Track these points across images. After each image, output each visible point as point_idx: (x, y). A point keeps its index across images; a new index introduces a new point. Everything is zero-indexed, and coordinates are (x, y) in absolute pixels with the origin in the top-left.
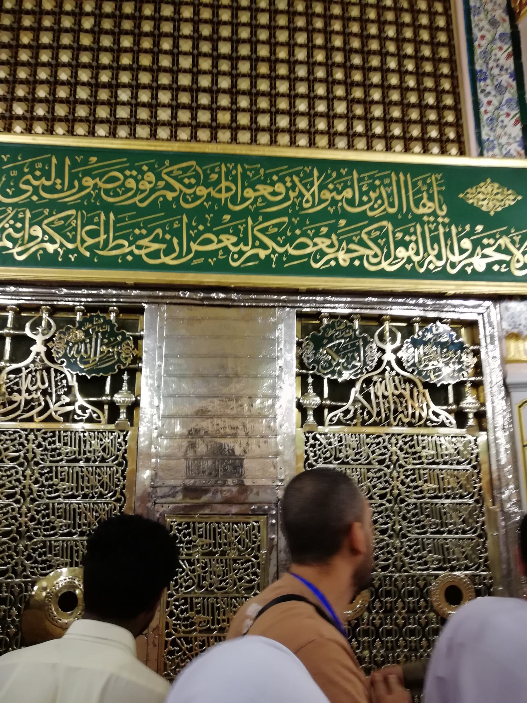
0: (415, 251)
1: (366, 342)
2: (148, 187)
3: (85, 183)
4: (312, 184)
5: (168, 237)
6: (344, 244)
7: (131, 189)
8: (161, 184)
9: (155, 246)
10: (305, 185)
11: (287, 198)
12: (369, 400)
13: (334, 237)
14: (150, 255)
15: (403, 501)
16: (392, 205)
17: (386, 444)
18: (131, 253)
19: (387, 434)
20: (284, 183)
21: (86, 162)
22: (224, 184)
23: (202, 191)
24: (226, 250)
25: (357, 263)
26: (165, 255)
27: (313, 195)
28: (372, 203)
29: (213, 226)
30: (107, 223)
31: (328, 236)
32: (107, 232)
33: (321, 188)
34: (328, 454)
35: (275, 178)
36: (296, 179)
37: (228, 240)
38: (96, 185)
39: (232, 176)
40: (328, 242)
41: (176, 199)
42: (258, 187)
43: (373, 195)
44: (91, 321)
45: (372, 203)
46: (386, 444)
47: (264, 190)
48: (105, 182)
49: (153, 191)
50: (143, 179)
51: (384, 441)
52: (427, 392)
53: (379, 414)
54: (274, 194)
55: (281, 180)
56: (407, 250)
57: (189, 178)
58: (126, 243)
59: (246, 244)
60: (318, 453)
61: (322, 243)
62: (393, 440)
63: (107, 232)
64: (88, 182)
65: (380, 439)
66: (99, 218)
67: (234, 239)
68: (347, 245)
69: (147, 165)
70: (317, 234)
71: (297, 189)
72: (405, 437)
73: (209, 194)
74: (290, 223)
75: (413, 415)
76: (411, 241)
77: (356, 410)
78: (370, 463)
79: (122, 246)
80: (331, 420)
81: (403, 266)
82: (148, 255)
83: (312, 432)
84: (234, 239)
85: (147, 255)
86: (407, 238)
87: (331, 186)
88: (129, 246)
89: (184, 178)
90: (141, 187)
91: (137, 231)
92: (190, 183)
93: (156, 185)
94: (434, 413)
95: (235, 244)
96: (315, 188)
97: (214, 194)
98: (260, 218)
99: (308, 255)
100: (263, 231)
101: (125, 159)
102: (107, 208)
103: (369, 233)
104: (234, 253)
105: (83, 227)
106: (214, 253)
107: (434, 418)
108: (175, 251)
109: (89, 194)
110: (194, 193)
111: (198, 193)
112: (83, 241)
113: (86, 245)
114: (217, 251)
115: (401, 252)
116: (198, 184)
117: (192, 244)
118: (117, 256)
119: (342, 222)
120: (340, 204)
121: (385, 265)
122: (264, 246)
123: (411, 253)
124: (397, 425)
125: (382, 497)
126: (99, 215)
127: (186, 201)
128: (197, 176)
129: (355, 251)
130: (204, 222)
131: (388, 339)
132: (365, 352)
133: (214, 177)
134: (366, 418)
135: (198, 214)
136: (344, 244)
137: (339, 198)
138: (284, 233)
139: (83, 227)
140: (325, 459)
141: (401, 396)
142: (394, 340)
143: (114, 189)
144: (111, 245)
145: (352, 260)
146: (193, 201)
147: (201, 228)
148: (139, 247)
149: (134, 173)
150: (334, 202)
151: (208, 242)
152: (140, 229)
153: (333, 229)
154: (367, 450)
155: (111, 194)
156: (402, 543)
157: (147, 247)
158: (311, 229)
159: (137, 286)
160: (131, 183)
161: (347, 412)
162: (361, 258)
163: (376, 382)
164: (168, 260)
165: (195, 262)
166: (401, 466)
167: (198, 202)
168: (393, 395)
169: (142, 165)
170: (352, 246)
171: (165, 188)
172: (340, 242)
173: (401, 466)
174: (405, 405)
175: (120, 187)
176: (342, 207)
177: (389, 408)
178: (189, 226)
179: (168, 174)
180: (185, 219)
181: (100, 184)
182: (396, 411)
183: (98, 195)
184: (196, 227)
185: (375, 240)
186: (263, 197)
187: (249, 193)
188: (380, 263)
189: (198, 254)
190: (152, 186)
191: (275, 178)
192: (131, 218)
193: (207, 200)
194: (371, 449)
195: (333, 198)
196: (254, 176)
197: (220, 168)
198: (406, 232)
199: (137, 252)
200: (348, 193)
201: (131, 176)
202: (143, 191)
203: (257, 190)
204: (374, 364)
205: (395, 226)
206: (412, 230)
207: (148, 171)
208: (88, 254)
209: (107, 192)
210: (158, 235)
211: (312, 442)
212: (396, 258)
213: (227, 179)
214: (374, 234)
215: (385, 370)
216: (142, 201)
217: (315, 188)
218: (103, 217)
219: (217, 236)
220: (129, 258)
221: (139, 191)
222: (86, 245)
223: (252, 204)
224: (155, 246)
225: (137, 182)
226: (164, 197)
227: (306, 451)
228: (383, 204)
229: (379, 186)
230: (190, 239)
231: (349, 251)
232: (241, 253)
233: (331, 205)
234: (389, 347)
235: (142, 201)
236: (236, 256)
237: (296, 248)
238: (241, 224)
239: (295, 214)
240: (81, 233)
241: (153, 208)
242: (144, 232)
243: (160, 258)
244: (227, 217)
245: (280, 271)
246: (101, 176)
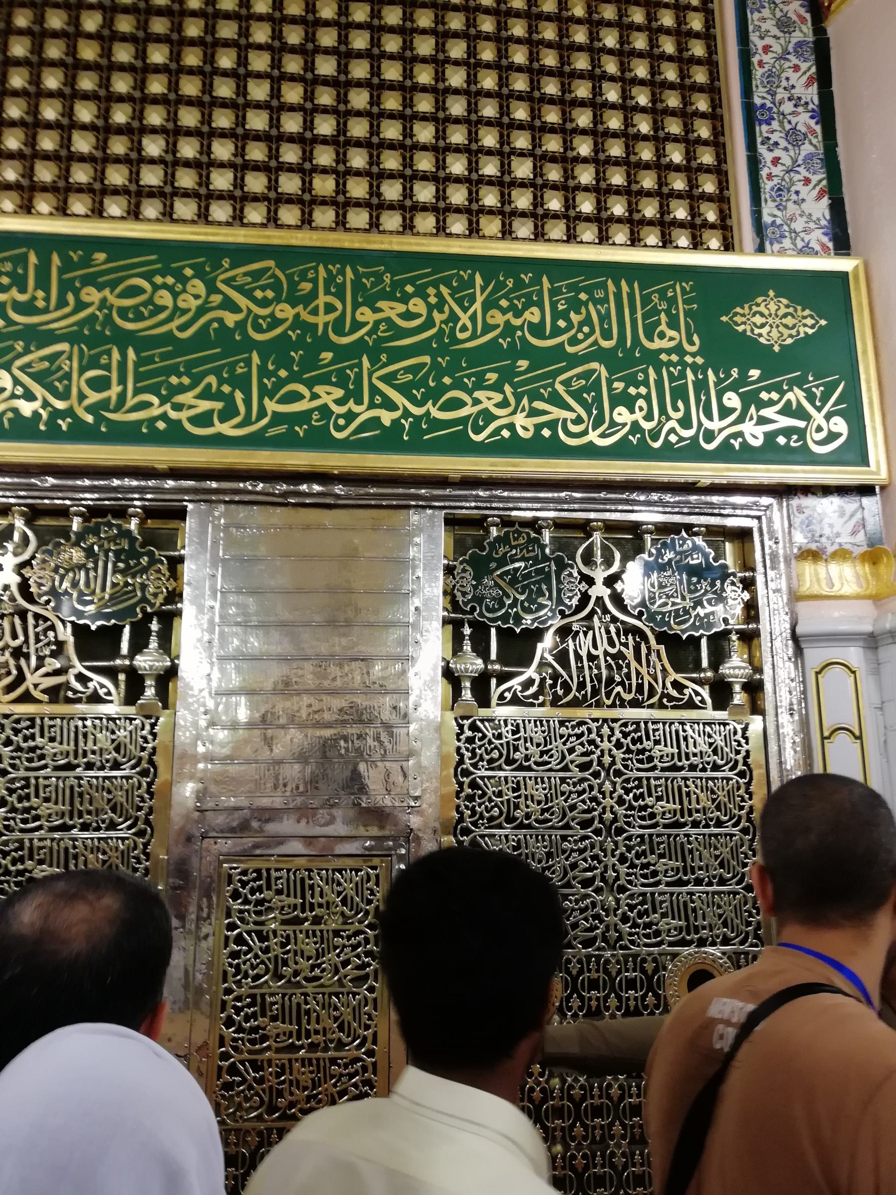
0: (644, 413)
1: (561, 566)
2: (194, 304)
3: (85, 298)
4: (472, 300)
5: (226, 389)
6: (525, 401)
7: (164, 308)
8: (216, 299)
9: (205, 405)
10: (459, 302)
11: (429, 323)
12: (565, 665)
13: (508, 389)
14: (196, 420)
15: (620, 831)
16: (607, 335)
17: (593, 736)
18: (164, 417)
19: (595, 720)
20: (425, 297)
21: (87, 262)
22: (322, 299)
23: (285, 311)
24: (325, 411)
25: (546, 433)
26: (222, 420)
27: (473, 318)
28: (573, 332)
29: (304, 370)
30: (122, 365)
31: (497, 387)
32: (122, 381)
33: (488, 305)
34: (495, 755)
35: (409, 289)
36: (445, 291)
37: (329, 395)
38: (104, 300)
39: (337, 285)
40: (498, 397)
41: (241, 325)
42: (381, 304)
43: (575, 318)
44: (96, 532)
45: (573, 332)
46: (593, 736)
47: (391, 310)
48: (121, 296)
49: (202, 311)
50: (184, 291)
51: (590, 731)
52: (662, 648)
53: (582, 686)
54: (408, 316)
55: (421, 293)
56: (632, 412)
57: (263, 288)
58: (155, 400)
59: (359, 402)
61: (488, 400)
62: (606, 730)
63: (122, 381)
64: (91, 295)
65: (584, 728)
66: (110, 358)
67: (339, 393)
68: (530, 402)
69: (191, 266)
70: (480, 385)
71: (446, 308)
72: (625, 725)
73: (297, 315)
74: (435, 365)
75: (640, 687)
76: (639, 396)
77: (543, 680)
78: (566, 769)
79: (149, 405)
80: (501, 697)
81: (625, 438)
82: (193, 420)
83: (468, 718)
84: (339, 393)
85: (191, 420)
86: (632, 391)
87: (504, 303)
88: (161, 405)
89: (255, 289)
90: (181, 304)
91: (174, 380)
92: (265, 298)
93: (206, 302)
94: (676, 685)
95: (340, 402)
96: (478, 306)
97: (305, 316)
98: (384, 358)
99: (464, 420)
100: (388, 379)
101: (153, 257)
102: (124, 339)
103: (566, 383)
104: (339, 416)
105: (82, 371)
106: (304, 417)
107: (674, 693)
108: (238, 414)
109: (93, 317)
110: (272, 315)
111: (279, 315)
112: (82, 397)
113: (86, 402)
114: (310, 411)
115: (622, 415)
116: (278, 300)
117: (266, 401)
118: (139, 423)
119: (523, 364)
120: (519, 333)
121: (593, 437)
122: (390, 406)
123: (638, 416)
124: (613, 705)
125: (585, 824)
126: (109, 353)
127: (258, 329)
128: (276, 286)
129: (545, 413)
130: (286, 363)
131: (599, 560)
132: (559, 582)
133: (307, 286)
134: (560, 692)
135: (277, 350)
136: (525, 401)
137: (517, 322)
138: (423, 382)
139: (82, 371)
141: (620, 656)
142: (608, 563)
143: (136, 308)
144: (130, 403)
145: (538, 427)
146: (271, 328)
147: (283, 373)
148: (178, 407)
149: (170, 280)
150: (509, 330)
151: (296, 397)
152: (179, 376)
153: (507, 375)
154: (561, 747)
155: (131, 316)
156: (618, 901)
157: (191, 407)
158: (469, 377)
159: (175, 473)
160: (165, 298)
162: (552, 425)
163: (577, 633)
164: (226, 429)
165: (272, 432)
166: (618, 773)
167: (278, 331)
168: (606, 653)
169: (183, 267)
170: (539, 405)
171: (221, 307)
172: (518, 398)
173: (618, 773)
174: (625, 670)
175: (145, 304)
176: (523, 339)
177: (599, 677)
178: (263, 372)
179: (227, 282)
180: (256, 359)
181: (112, 299)
182: (610, 681)
183: (108, 317)
184: (274, 373)
185: (576, 395)
186: (388, 320)
187: (366, 315)
188: (585, 433)
189: (278, 418)
190: (199, 302)
191: (409, 289)
192: (164, 357)
193: (292, 327)
194: (569, 745)
195: (507, 322)
196: (374, 285)
197: (317, 272)
198: (631, 381)
199: (173, 415)
200: (533, 315)
201: (165, 286)
202: (185, 311)
203: (380, 310)
204: (575, 602)
205: (611, 372)
206: (641, 377)
207: (193, 277)
208: (90, 419)
209: (123, 313)
210: (209, 385)
211: (468, 733)
212: (613, 424)
213: (327, 292)
214: (576, 385)
215: (593, 612)
216: (182, 328)
217: (478, 306)
218: (116, 355)
219: (310, 389)
220: (161, 425)
221: (178, 311)
222: (86, 402)
223: (369, 334)
224: (205, 405)
225: (175, 295)
226: (220, 321)
227: (459, 748)
228: (592, 332)
229: (586, 304)
230: (264, 392)
231: (533, 413)
232: (350, 416)
233: (502, 335)
234: (600, 574)
235: (182, 328)
236: (341, 422)
237: (443, 408)
238: (351, 368)
239: (443, 350)
240: (79, 383)
241: (201, 340)
242: (186, 381)
243: (212, 425)
244: (327, 356)
245: (417, 446)
246: (113, 285)
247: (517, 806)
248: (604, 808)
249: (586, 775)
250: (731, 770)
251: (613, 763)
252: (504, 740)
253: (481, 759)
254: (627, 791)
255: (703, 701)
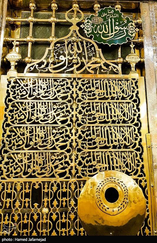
19: (70, 78)
34: (24, 93)
52: (100, 50)
60: (15, 116)
65: (65, 82)
72: (83, 81)
78: (56, 99)
94: (107, 65)
140: (22, 96)
154: (54, 90)
161: (42, 63)
166: (79, 101)
173: (79, 101)
247: (33, 115)
248: (73, 115)
249: (65, 101)
250: (130, 99)
251: (78, 96)
252: (29, 87)
253: (16, 119)
254: (83, 108)
255: (117, 70)
